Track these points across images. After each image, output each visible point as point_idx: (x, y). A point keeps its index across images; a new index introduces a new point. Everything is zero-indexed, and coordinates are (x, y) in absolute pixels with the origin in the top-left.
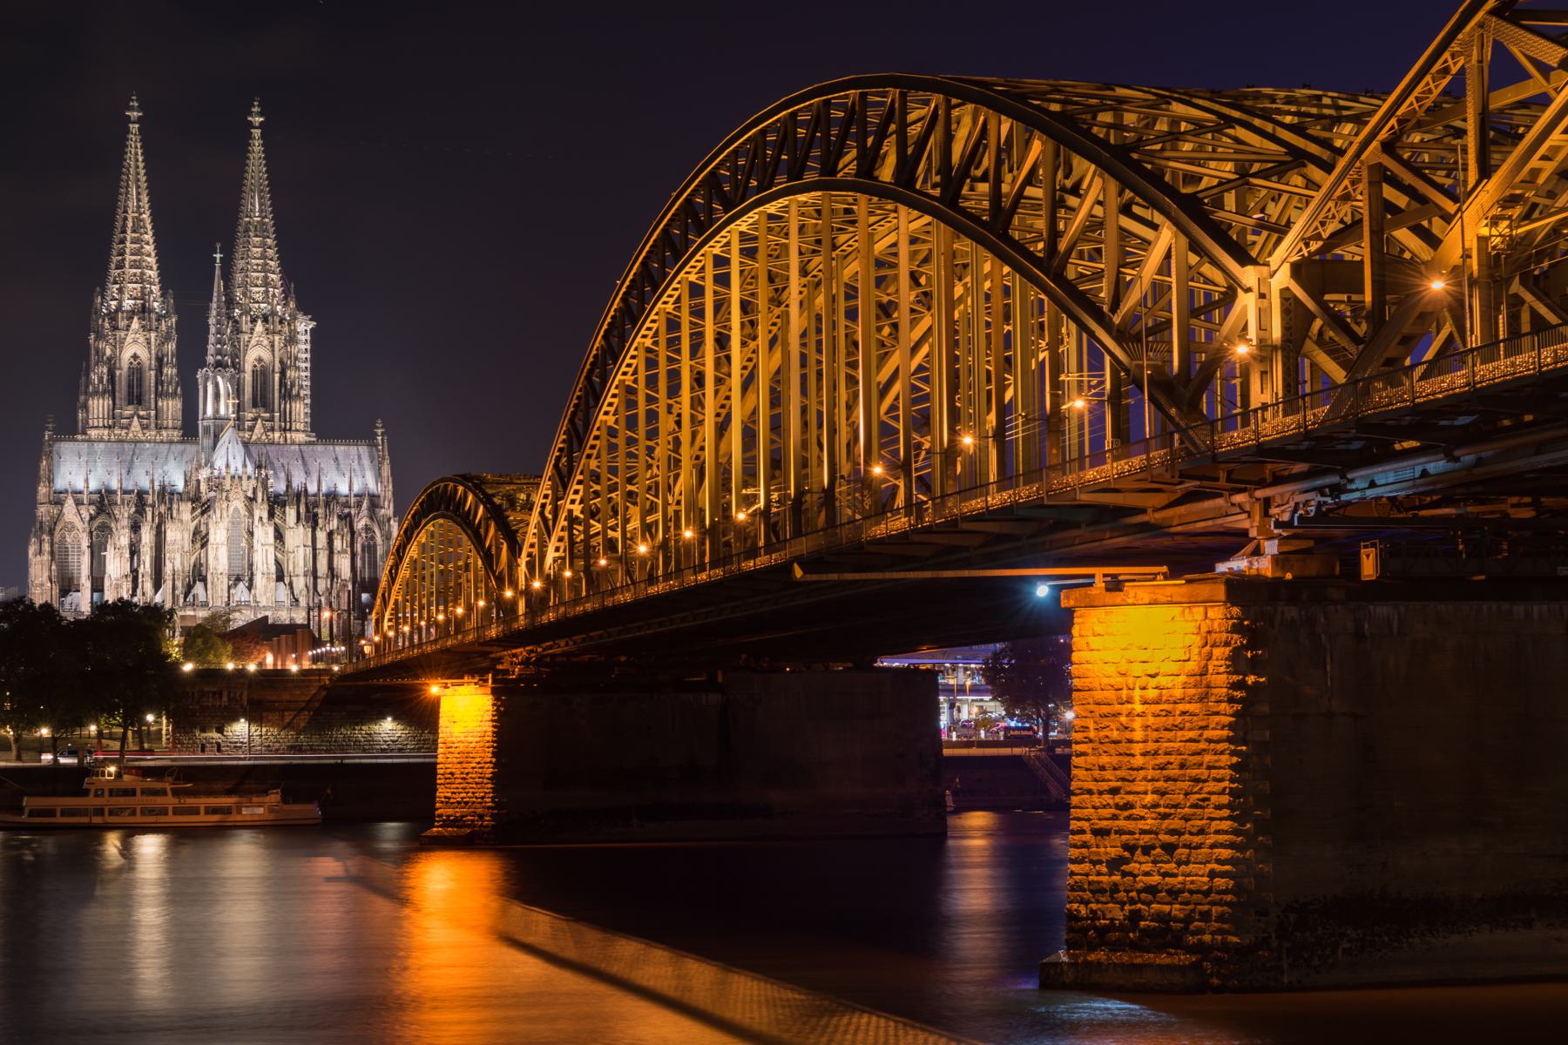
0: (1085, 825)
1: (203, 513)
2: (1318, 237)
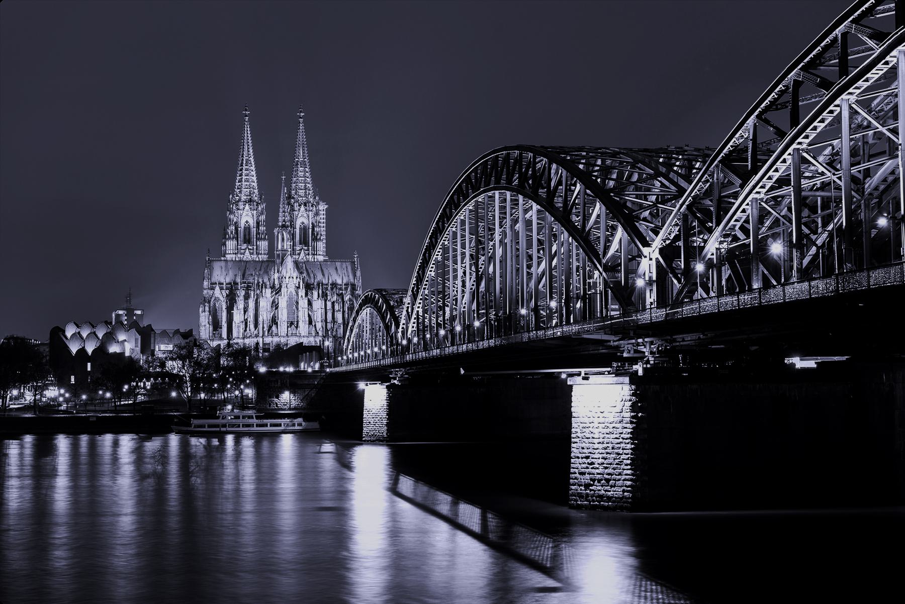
0: (576, 471)
2: (668, 239)
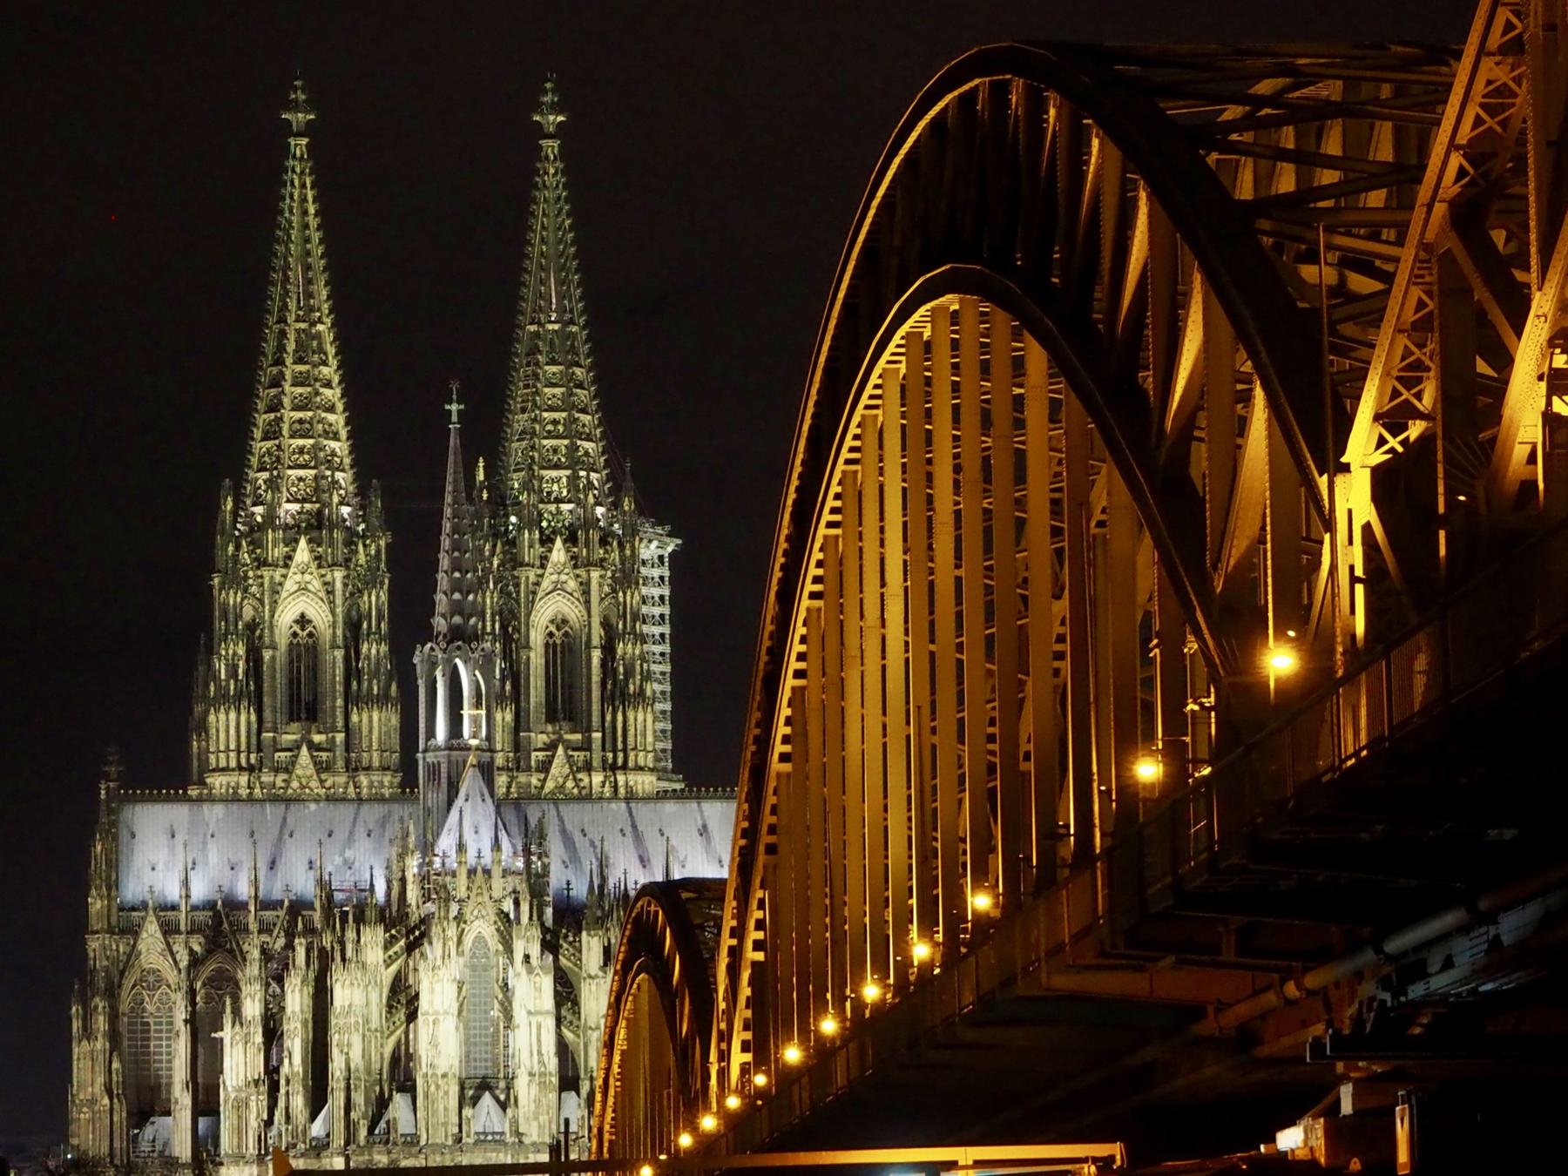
1: (410, 948)
